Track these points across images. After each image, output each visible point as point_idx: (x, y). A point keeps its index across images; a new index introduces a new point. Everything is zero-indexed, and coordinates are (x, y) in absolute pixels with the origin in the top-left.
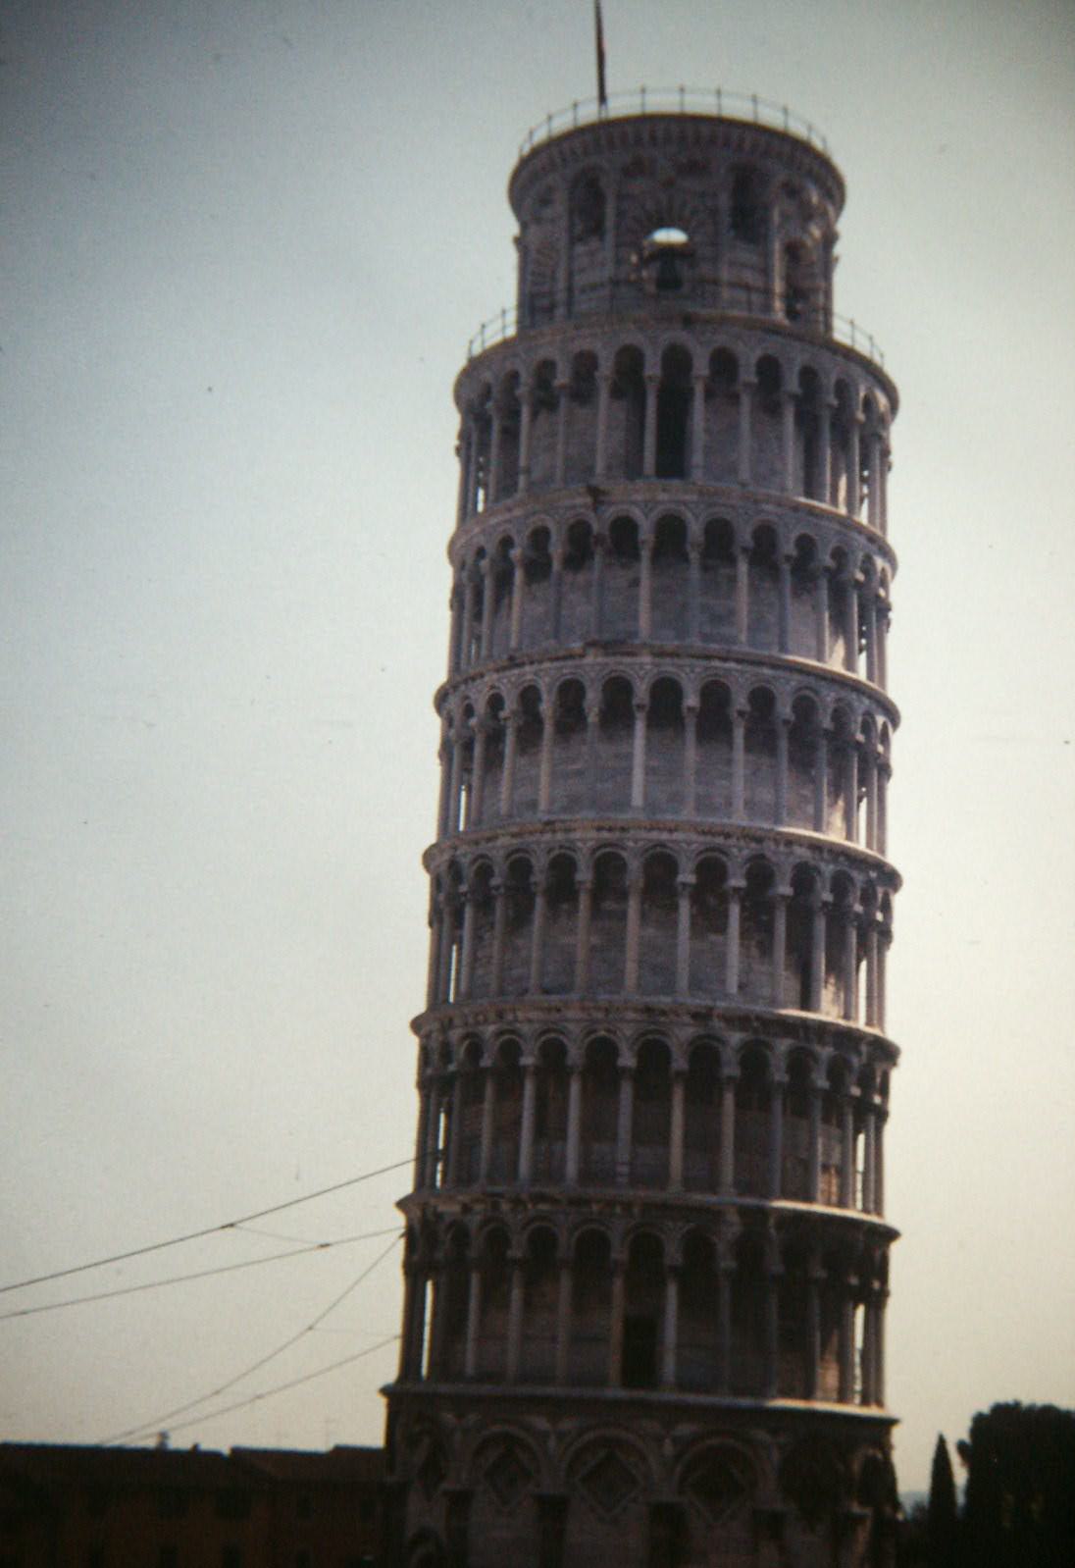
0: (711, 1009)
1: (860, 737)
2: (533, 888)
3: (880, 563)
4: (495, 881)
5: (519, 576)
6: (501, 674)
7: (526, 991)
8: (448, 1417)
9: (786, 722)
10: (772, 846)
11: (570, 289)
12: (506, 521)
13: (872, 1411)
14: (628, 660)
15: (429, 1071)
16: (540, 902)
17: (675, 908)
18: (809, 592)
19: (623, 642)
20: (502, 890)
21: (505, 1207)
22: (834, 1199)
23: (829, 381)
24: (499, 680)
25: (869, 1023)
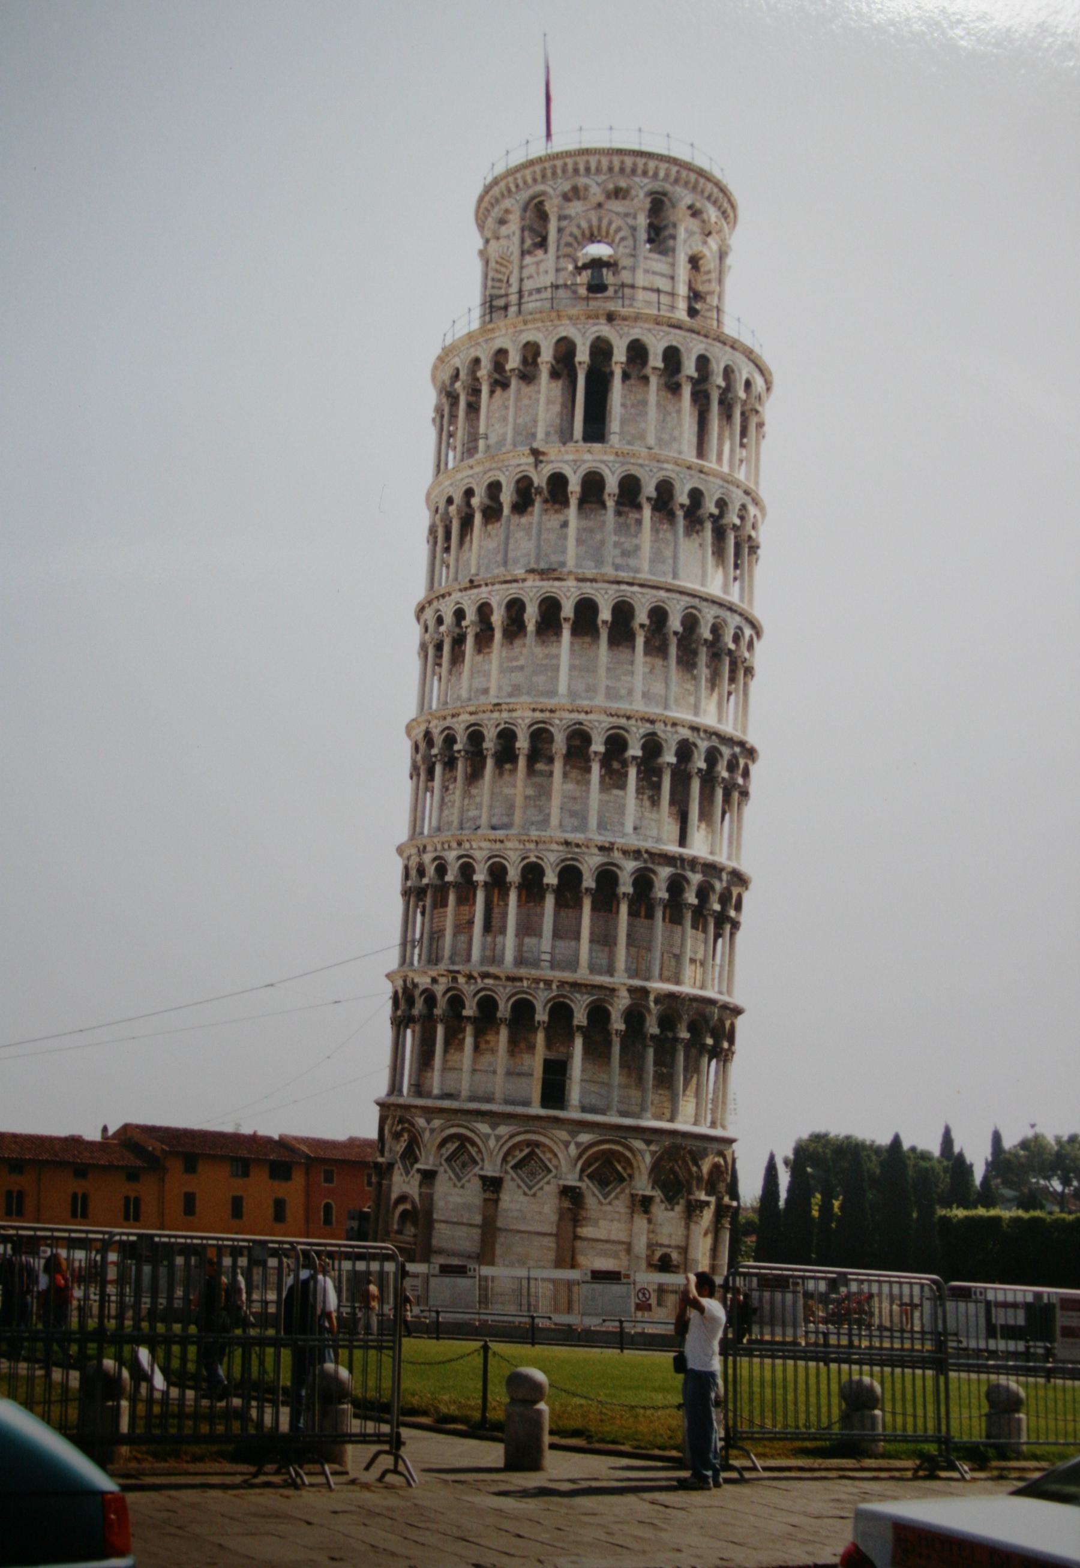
0: (612, 844)
2: (485, 752)
3: (752, 510)
4: (457, 747)
5: (478, 518)
6: (464, 593)
7: (479, 827)
9: (676, 633)
10: (662, 726)
11: (520, 292)
14: (557, 584)
15: (409, 883)
16: (490, 763)
17: (588, 770)
18: (697, 532)
19: (554, 570)
20: (463, 753)
21: (461, 980)
24: (462, 597)
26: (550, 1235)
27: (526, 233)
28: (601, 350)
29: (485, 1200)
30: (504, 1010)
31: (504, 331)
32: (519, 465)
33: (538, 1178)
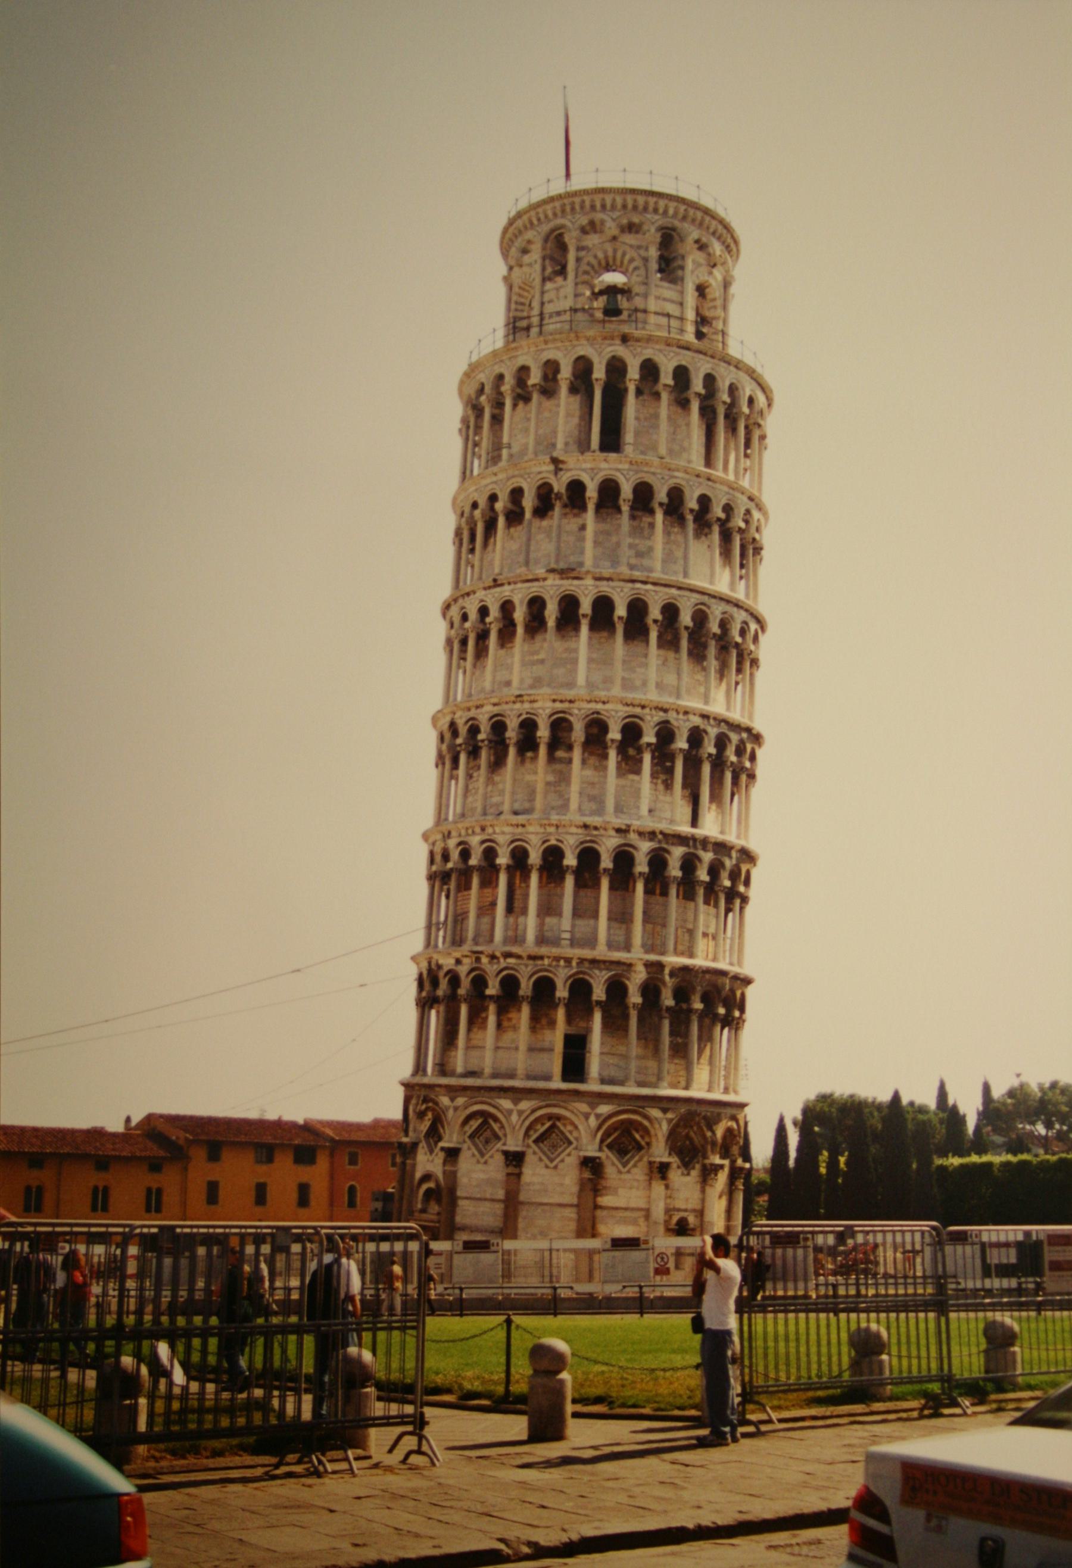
0: (629, 826)
1: (739, 639)
2: (508, 741)
3: (756, 515)
4: (481, 737)
5: (501, 521)
6: (488, 591)
7: (501, 813)
8: (445, 1100)
9: (687, 628)
10: (674, 714)
11: (541, 315)
12: (495, 483)
13: (730, 1098)
14: (576, 582)
15: (434, 868)
16: (512, 752)
17: (605, 757)
18: (706, 535)
19: (573, 570)
20: (486, 742)
21: (485, 960)
22: (710, 956)
23: (723, 385)
24: (486, 595)
25: (738, 837)
26: (571, 1206)
27: (547, 262)
28: (616, 368)
29: (508, 1174)
30: (526, 988)
31: (526, 350)
32: (540, 473)
33: (560, 1150)
